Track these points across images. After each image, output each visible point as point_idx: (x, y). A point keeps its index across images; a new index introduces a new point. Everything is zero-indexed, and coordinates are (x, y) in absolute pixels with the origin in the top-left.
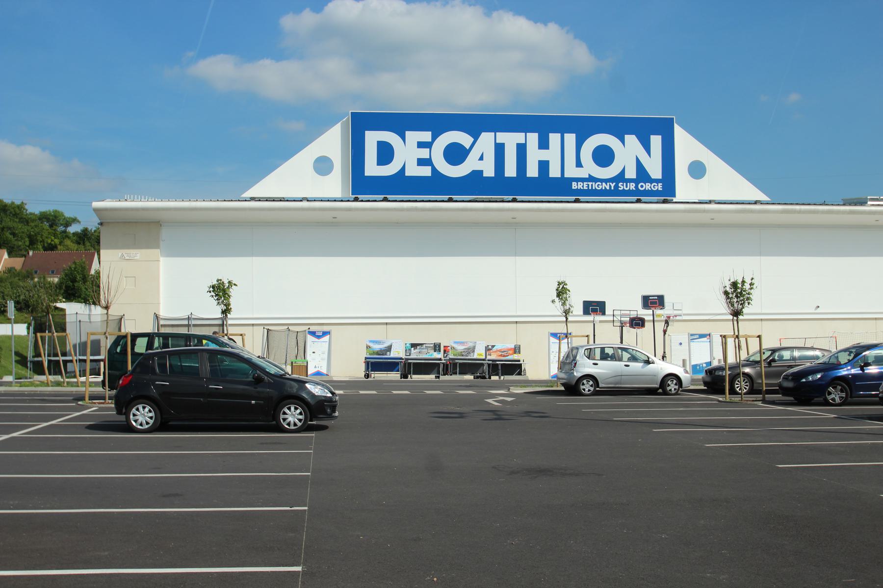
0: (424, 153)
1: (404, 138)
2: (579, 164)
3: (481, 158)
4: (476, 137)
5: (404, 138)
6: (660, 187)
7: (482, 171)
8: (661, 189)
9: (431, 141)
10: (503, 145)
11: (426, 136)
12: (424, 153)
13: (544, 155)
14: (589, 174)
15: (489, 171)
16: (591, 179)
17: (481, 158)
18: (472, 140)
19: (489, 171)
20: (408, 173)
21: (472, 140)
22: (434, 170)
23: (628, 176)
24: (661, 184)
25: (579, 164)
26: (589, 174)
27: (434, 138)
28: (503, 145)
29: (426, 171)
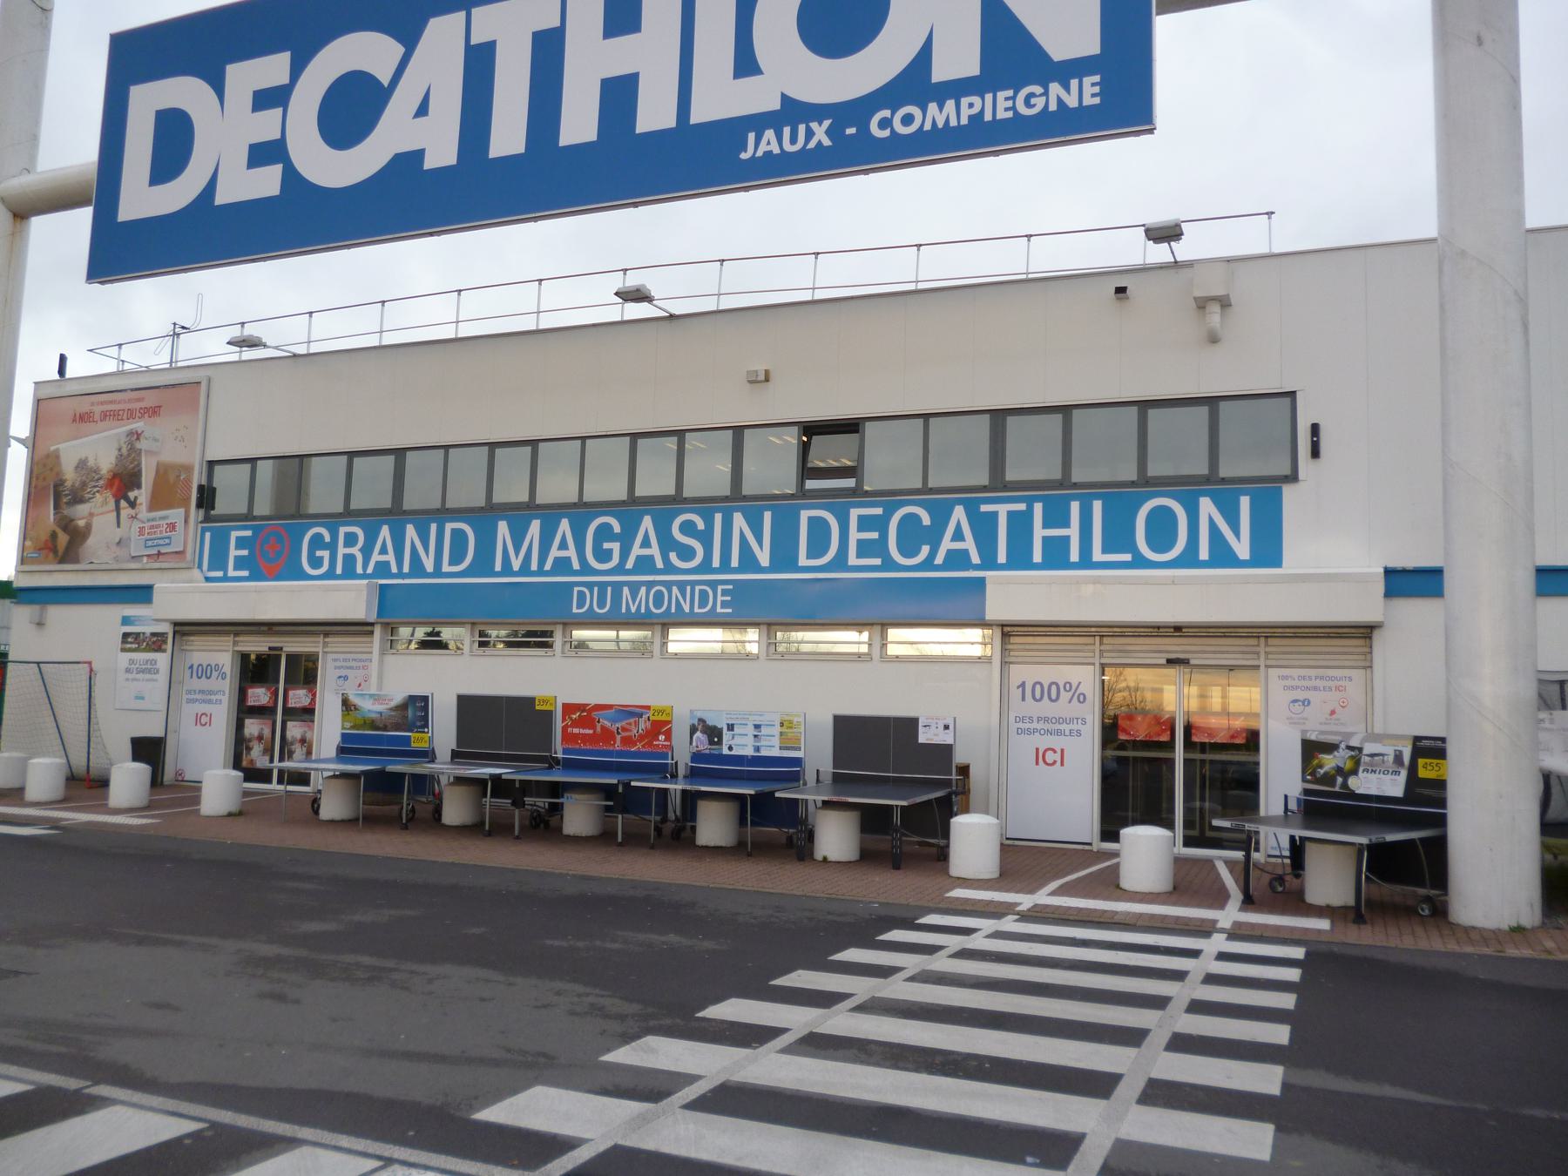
0: (266, 126)
1: (219, 88)
2: (746, 64)
3: (422, 110)
4: (409, 39)
5: (219, 88)
6: (1087, 92)
7: (419, 154)
8: (1097, 100)
9: (284, 79)
10: (489, 48)
11: (272, 69)
12: (266, 126)
13: (621, 56)
14: (784, 97)
15: (442, 152)
16: (793, 112)
17: (422, 110)
18: (399, 50)
19: (442, 152)
20: (221, 199)
21: (400, 50)
22: (291, 177)
23: (941, 72)
24: (1097, 78)
25: (746, 64)
26: (784, 97)
27: (297, 69)
28: (489, 48)
29: (267, 182)
